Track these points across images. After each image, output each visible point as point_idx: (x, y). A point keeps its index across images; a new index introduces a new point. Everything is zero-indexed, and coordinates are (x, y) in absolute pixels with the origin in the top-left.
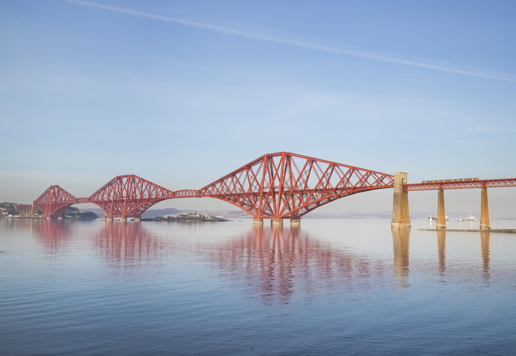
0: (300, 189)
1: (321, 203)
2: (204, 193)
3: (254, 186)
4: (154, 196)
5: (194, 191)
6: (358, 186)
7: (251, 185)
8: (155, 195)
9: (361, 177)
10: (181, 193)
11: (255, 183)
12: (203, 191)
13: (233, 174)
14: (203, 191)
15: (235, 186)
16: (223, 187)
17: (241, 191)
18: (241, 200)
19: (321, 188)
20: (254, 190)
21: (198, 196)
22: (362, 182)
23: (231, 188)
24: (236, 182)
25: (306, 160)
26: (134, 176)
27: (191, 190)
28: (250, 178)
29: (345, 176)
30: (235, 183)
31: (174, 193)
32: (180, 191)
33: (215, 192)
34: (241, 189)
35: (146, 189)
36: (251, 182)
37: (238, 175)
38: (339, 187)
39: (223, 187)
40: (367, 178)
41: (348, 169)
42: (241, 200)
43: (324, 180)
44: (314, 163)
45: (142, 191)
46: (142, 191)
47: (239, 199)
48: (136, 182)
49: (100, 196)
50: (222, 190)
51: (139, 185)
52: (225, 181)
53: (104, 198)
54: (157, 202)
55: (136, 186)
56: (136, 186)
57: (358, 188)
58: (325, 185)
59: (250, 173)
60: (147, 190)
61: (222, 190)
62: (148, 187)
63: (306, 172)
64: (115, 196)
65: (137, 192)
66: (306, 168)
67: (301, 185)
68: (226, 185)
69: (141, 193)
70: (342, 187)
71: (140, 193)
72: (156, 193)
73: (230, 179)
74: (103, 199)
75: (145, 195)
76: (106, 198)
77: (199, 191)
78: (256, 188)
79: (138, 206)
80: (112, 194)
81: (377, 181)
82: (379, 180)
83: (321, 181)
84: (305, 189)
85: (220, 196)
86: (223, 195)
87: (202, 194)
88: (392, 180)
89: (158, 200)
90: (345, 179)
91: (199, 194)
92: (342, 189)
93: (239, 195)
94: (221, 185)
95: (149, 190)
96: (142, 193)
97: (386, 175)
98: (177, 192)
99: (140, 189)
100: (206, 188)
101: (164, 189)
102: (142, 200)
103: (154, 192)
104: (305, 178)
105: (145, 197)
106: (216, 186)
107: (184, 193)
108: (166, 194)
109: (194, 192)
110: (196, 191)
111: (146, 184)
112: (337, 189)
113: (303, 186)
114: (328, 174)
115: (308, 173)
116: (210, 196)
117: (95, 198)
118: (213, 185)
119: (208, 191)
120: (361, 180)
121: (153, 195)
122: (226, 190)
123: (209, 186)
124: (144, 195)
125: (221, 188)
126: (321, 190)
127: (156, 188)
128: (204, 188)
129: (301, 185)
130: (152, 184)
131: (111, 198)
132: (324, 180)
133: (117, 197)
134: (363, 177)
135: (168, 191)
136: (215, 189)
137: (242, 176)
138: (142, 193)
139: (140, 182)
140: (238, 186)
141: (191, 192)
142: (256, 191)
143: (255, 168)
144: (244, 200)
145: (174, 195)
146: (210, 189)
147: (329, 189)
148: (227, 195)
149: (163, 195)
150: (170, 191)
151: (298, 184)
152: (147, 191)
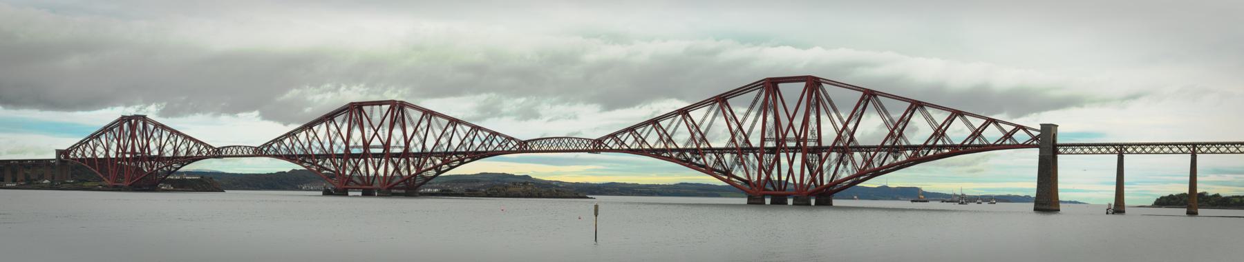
0: (414, 150)
1: (442, 170)
2: (266, 152)
3: (337, 144)
4: (183, 154)
5: (251, 147)
6: (480, 150)
7: (332, 143)
8: (185, 151)
9: (483, 139)
10: (229, 150)
11: (339, 141)
12: (265, 149)
13: (309, 126)
14: (265, 149)
15: (310, 144)
16: (293, 145)
17: (320, 151)
18: (320, 163)
19: (438, 151)
20: (337, 151)
21: (254, 155)
22: (485, 146)
23: (306, 146)
24: (313, 138)
25: (421, 113)
26: (144, 118)
27: (240, 146)
28: (331, 133)
29: (467, 135)
30: (310, 139)
31: (218, 149)
32: (228, 147)
33: (282, 150)
34: (320, 147)
35: (168, 142)
36: (332, 139)
37: (315, 128)
38: (459, 150)
39: (293, 145)
40: (492, 141)
41: (470, 128)
42: (320, 163)
43: (444, 141)
44: (433, 118)
45: (160, 145)
46: (160, 145)
47: (318, 162)
48: (150, 130)
49: (88, 149)
50: (293, 147)
51: (155, 135)
52: (297, 135)
53: (97, 154)
54: (190, 163)
55: (149, 135)
56: (149, 135)
57: (480, 152)
58: (445, 147)
59: (332, 127)
60: (171, 143)
61: (293, 147)
62: (172, 139)
63: (422, 129)
64: (120, 151)
65: (153, 145)
66: (421, 124)
67: (416, 145)
68: (300, 142)
69: (160, 147)
70: (463, 150)
71: (157, 148)
72: (188, 148)
73: (304, 133)
74: (83, 154)
75: (168, 152)
76: (101, 153)
77: (259, 147)
78: (340, 147)
79: (155, 169)
80: (114, 146)
81: (500, 145)
82: (503, 144)
83: (438, 141)
84: (422, 151)
85: (290, 157)
86: (294, 156)
87: (264, 152)
88: (515, 144)
89: (190, 159)
90: (467, 140)
91: (259, 152)
92: (465, 153)
93: (318, 156)
94: (291, 141)
95: (174, 143)
96: (161, 149)
97: (511, 139)
98: (224, 148)
99: (158, 140)
100: (269, 145)
101: (202, 143)
102: (160, 158)
103: (183, 147)
104: (423, 137)
105: (167, 155)
106: (285, 142)
107: (234, 150)
108: (205, 150)
109: (251, 150)
110: (253, 149)
111: (169, 133)
112: (456, 153)
113: (420, 147)
114: (448, 134)
115: (425, 130)
116: (276, 156)
117: (76, 152)
118: (279, 140)
119: (271, 149)
120: (483, 143)
121: (182, 151)
122: (299, 148)
123: (275, 141)
124: (165, 151)
125: (291, 145)
126: (439, 153)
127: (186, 142)
128: (266, 144)
129: (416, 145)
130: (179, 133)
131: (112, 154)
132: (444, 141)
133: (124, 152)
134: (487, 138)
135: (206, 146)
136: (283, 146)
137: (321, 130)
138: (161, 149)
139: (158, 130)
140: (316, 144)
141: (245, 150)
142: (341, 152)
143: (339, 120)
144: (324, 162)
145: (218, 153)
146: (275, 145)
147: (451, 154)
148: (300, 156)
149: (199, 152)
150: (211, 147)
151: (412, 144)
152: (170, 145)
